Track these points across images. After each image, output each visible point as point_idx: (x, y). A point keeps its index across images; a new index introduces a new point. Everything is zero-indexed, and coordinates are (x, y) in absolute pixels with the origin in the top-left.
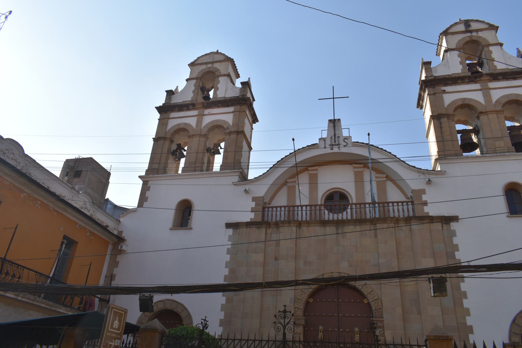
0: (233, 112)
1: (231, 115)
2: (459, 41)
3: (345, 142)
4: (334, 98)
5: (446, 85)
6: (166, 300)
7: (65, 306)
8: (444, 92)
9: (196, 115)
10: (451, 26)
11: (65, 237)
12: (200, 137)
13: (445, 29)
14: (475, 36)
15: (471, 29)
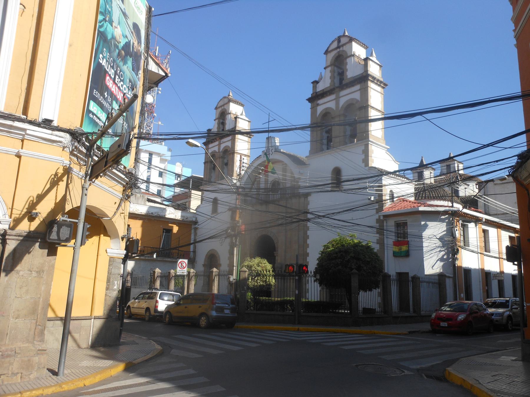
0: (231, 140)
1: (231, 141)
2: (333, 57)
3: (272, 151)
4: (269, 122)
5: (319, 99)
6: (212, 249)
7: (169, 258)
8: (318, 105)
9: (217, 144)
10: (330, 45)
11: (164, 229)
12: (220, 159)
13: (327, 49)
14: (341, 50)
15: (341, 44)
